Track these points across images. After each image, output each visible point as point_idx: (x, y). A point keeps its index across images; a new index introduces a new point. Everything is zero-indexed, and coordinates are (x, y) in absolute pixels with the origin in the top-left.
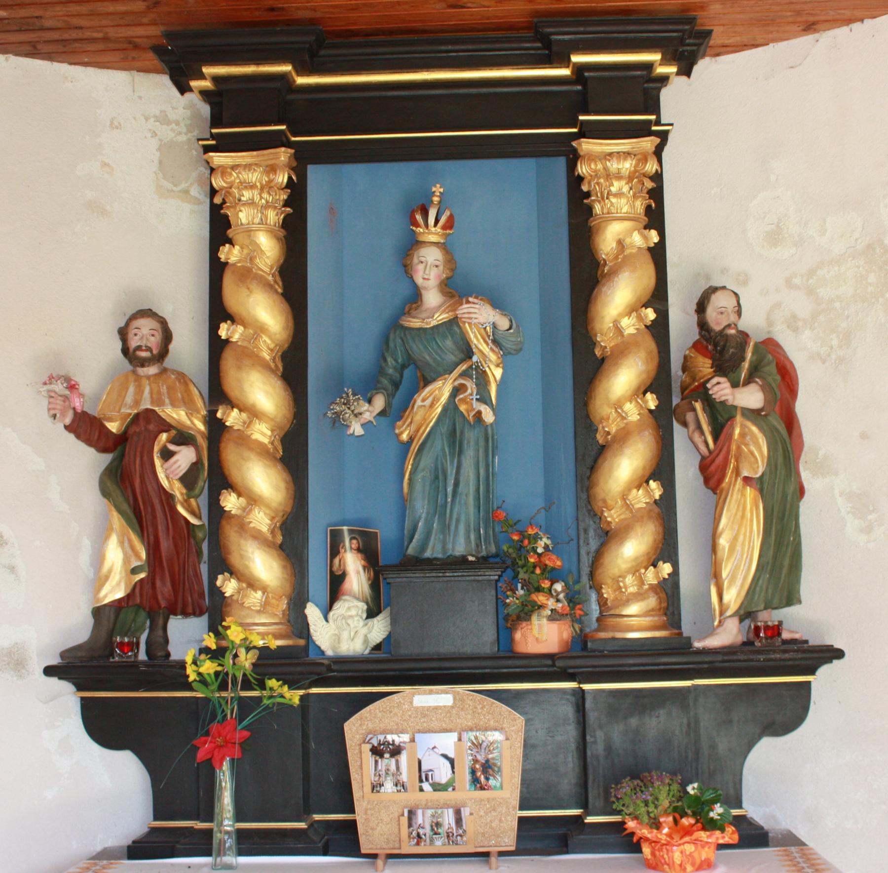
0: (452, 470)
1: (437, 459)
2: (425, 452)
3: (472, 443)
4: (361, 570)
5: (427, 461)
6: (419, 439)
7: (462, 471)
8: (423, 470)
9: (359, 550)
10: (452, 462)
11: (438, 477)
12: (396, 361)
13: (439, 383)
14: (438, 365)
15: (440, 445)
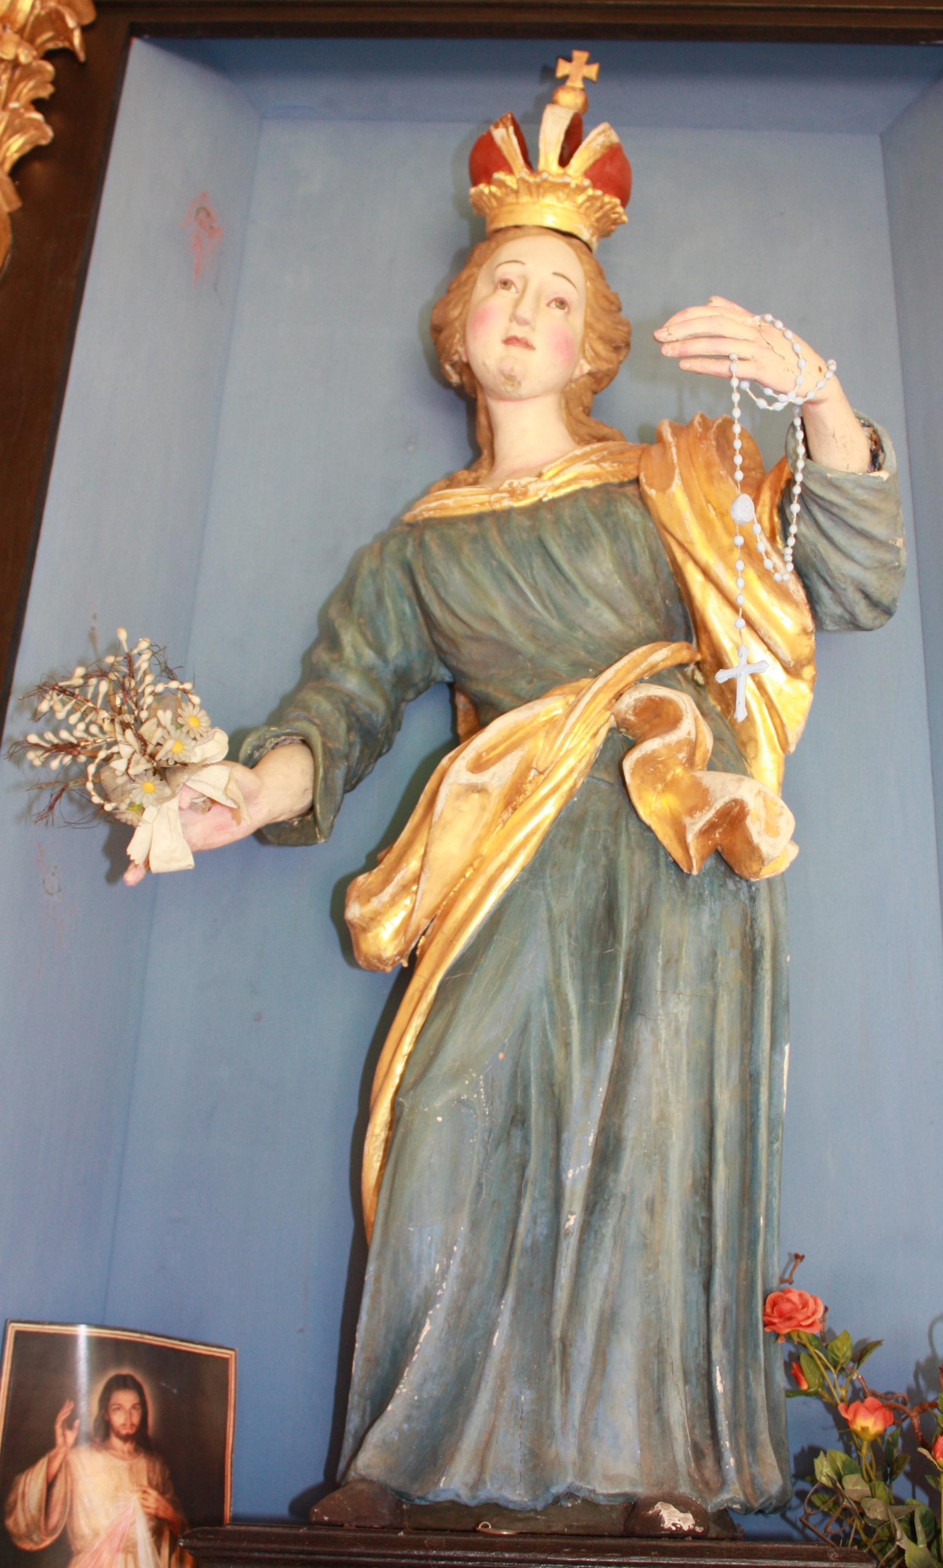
0: (592, 1083)
1: (524, 1030)
2: (472, 996)
3: (688, 965)
4: (142, 1533)
5: (481, 1032)
6: (451, 942)
7: (636, 1093)
8: (456, 1076)
9: (141, 1440)
10: (591, 1051)
11: (525, 1115)
12: (380, 651)
13: (552, 706)
14: (550, 650)
15: (544, 965)
